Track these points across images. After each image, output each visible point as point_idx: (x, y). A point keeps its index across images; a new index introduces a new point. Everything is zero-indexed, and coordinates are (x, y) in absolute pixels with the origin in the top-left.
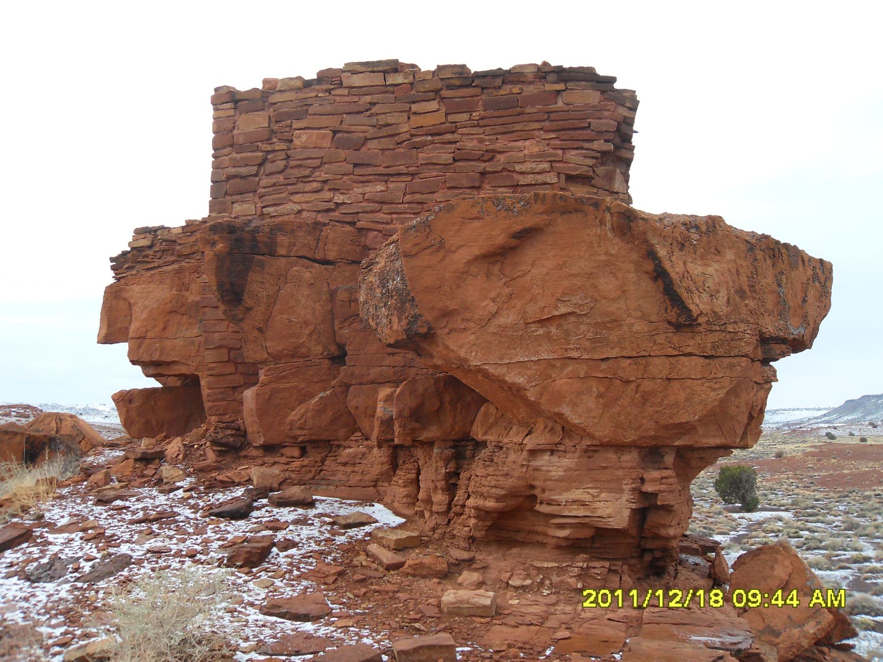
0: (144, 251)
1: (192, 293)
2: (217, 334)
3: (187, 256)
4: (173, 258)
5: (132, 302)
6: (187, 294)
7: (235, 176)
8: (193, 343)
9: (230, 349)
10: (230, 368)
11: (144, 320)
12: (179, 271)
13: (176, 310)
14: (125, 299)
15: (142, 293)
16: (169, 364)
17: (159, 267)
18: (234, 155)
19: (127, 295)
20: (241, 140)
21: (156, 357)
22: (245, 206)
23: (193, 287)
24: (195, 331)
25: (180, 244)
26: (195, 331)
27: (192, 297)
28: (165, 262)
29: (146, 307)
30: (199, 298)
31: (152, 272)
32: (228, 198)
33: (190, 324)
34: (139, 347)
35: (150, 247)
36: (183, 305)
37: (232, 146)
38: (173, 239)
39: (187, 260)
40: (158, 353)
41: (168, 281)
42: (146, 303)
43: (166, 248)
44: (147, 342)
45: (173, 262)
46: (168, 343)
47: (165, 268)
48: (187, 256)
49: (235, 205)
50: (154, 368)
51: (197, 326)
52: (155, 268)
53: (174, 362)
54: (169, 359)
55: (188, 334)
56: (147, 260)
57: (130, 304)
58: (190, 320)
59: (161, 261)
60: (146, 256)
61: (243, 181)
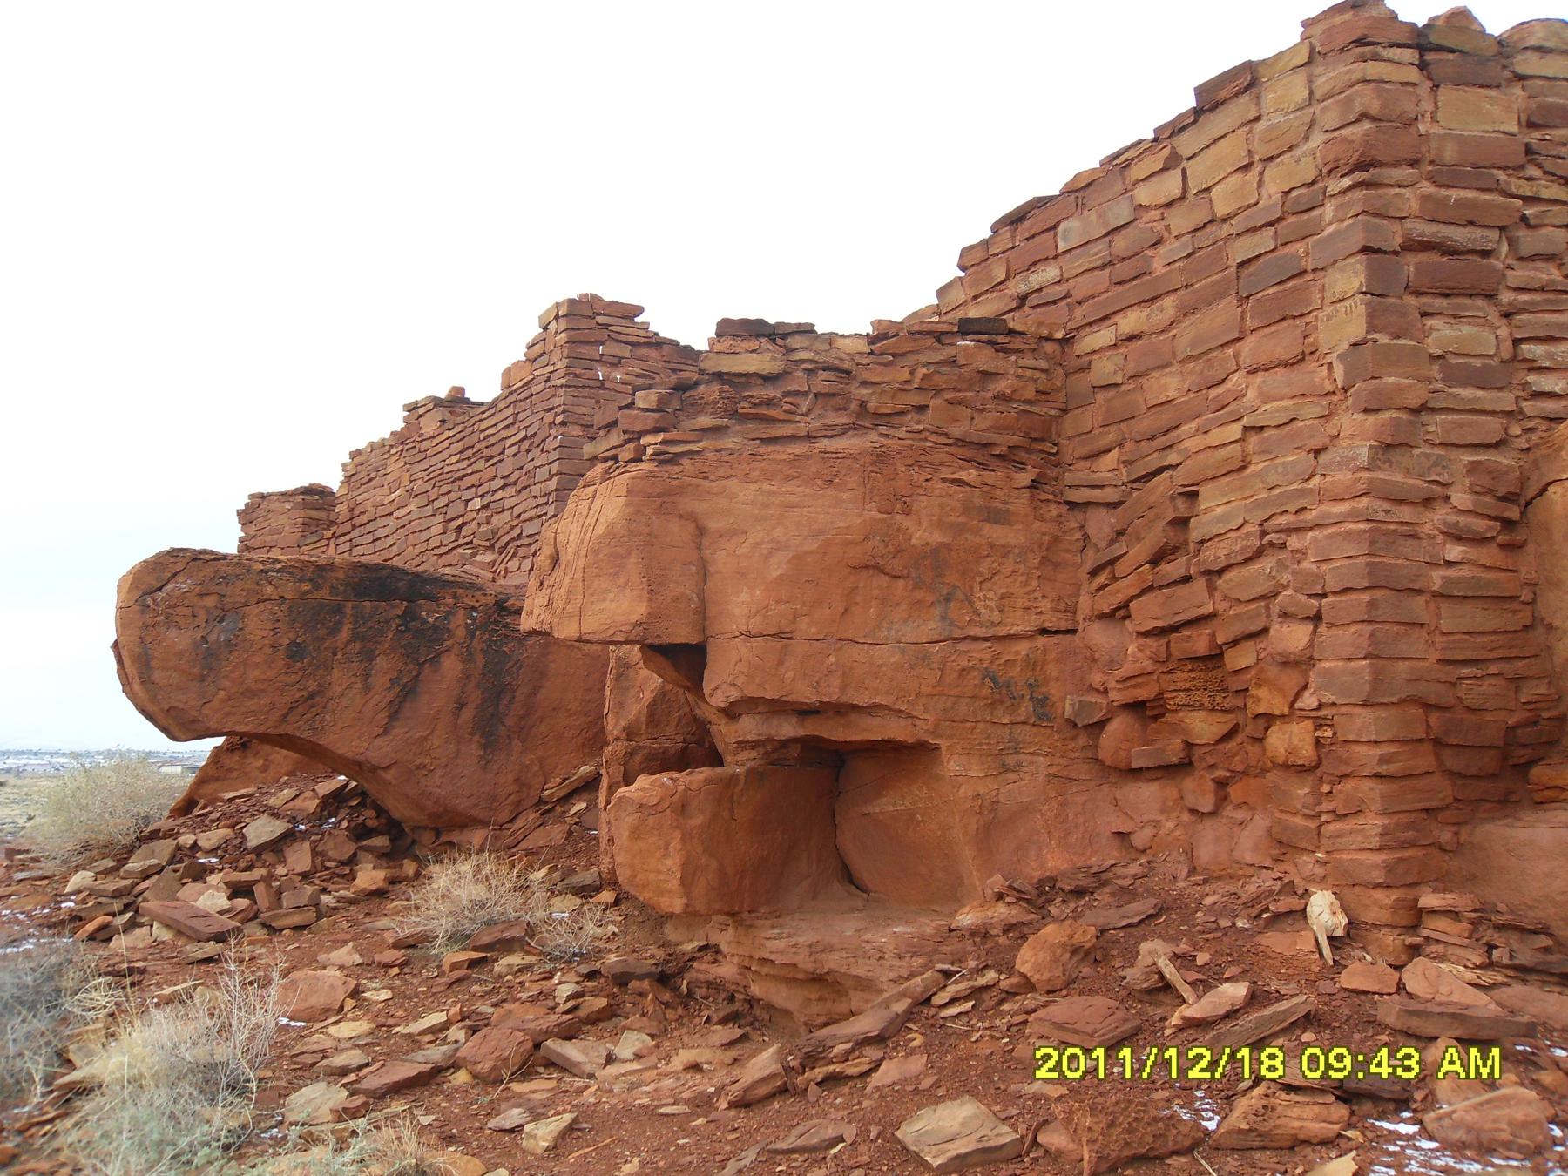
0: (747, 385)
1: (919, 523)
2: (1402, 666)
3: (880, 418)
4: (843, 420)
5: (713, 525)
6: (908, 522)
7: (1426, 246)
8: (924, 658)
9: (1427, 707)
10: (1424, 760)
11: (778, 582)
12: (880, 459)
13: (881, 564)
14: (692, 517)
15: (765, 506)
16: (841, 710)
17: (809, 437)
18: (1427, 188)
19: (699, 507)
20: (1450, 154)
21: (831, 694)
22: (1466, 330)
23: (920, 503)
24: (932, 626)
25: (865, 383)
26: (932, 626)
27: (922, 534)
28: (827, 427)
29: (779, 547)
30: (938, 537)
31: (798, 449)
32: (1411, 300)
33: (917, 603)
34: (781, 662)
35: (768, 379)
36: (899, 551)
37: (1414, 163)
38: (846, 365)
39: (884, 429)
40: (836, 682)
41: (853, 481)
42: (778, 533)
43: (835, 388)
44: (800, 648)
45: (844, 431)
46: (857, 654)
47: (826, 441)
48: (880, 418)
49: (1430, 322)
50: (794, 720)
51: (938, 610)
52: (794, 438)
53: (873, 709)
54: (863, 699)
55: (910, 632)
56: (772, 413)
57: (701, 531)
58: (919, 595)
59: (817, 424)
60: (770, 403)
61: (1455, 263)
